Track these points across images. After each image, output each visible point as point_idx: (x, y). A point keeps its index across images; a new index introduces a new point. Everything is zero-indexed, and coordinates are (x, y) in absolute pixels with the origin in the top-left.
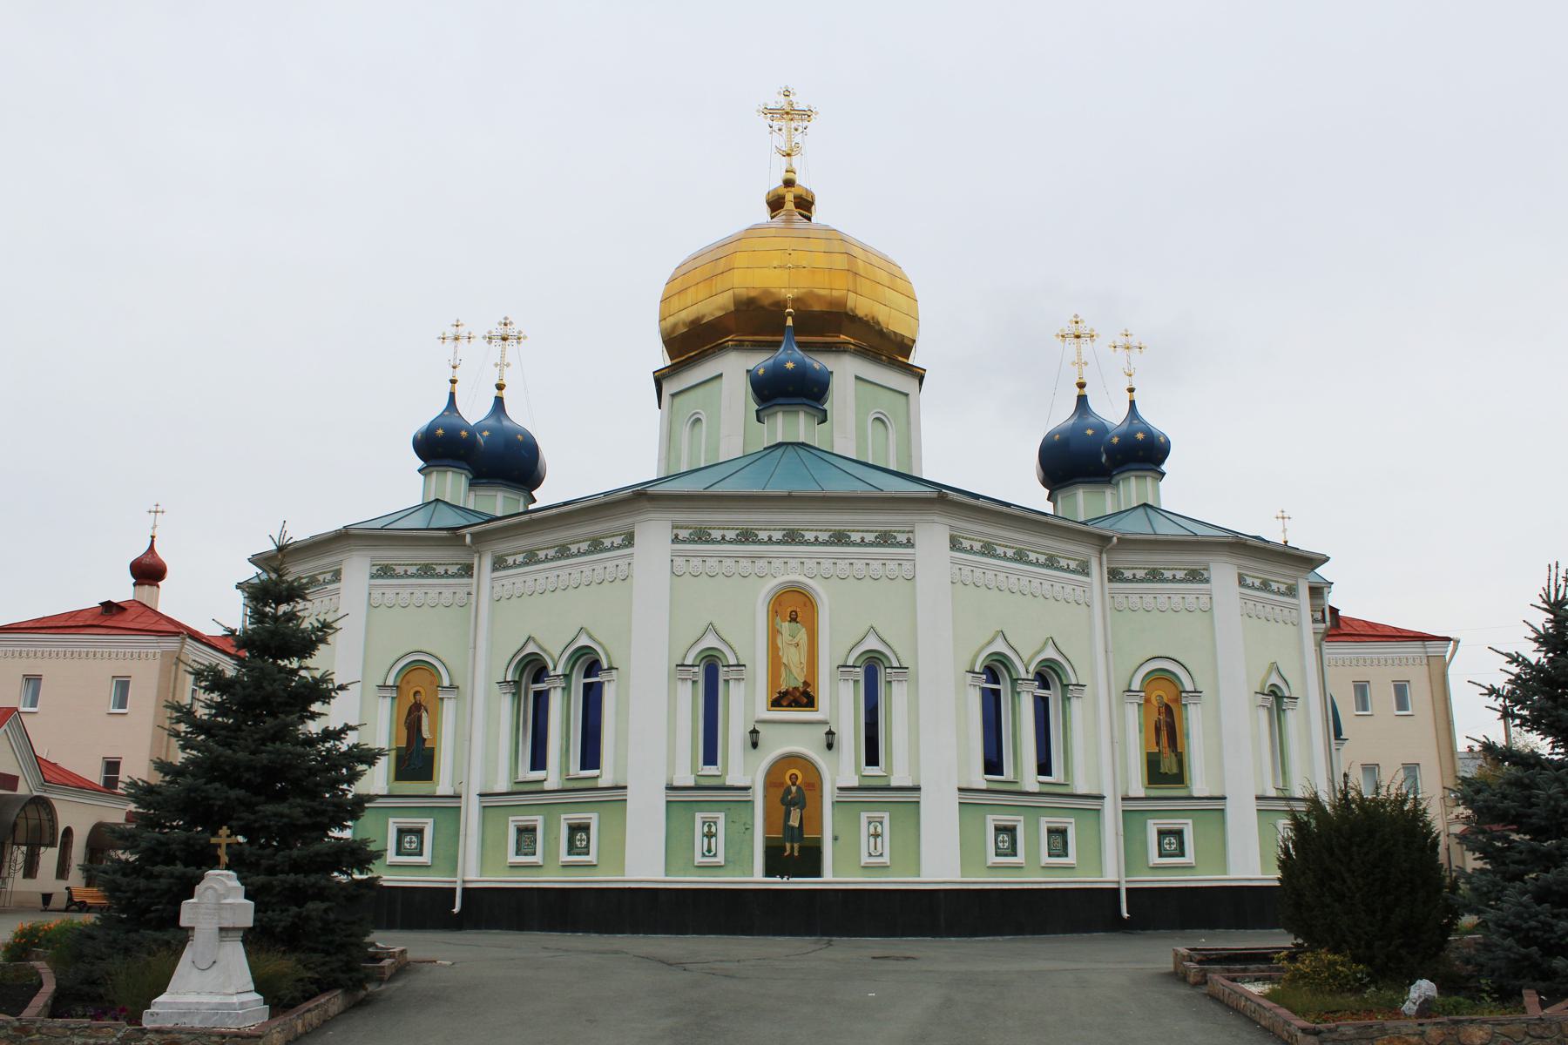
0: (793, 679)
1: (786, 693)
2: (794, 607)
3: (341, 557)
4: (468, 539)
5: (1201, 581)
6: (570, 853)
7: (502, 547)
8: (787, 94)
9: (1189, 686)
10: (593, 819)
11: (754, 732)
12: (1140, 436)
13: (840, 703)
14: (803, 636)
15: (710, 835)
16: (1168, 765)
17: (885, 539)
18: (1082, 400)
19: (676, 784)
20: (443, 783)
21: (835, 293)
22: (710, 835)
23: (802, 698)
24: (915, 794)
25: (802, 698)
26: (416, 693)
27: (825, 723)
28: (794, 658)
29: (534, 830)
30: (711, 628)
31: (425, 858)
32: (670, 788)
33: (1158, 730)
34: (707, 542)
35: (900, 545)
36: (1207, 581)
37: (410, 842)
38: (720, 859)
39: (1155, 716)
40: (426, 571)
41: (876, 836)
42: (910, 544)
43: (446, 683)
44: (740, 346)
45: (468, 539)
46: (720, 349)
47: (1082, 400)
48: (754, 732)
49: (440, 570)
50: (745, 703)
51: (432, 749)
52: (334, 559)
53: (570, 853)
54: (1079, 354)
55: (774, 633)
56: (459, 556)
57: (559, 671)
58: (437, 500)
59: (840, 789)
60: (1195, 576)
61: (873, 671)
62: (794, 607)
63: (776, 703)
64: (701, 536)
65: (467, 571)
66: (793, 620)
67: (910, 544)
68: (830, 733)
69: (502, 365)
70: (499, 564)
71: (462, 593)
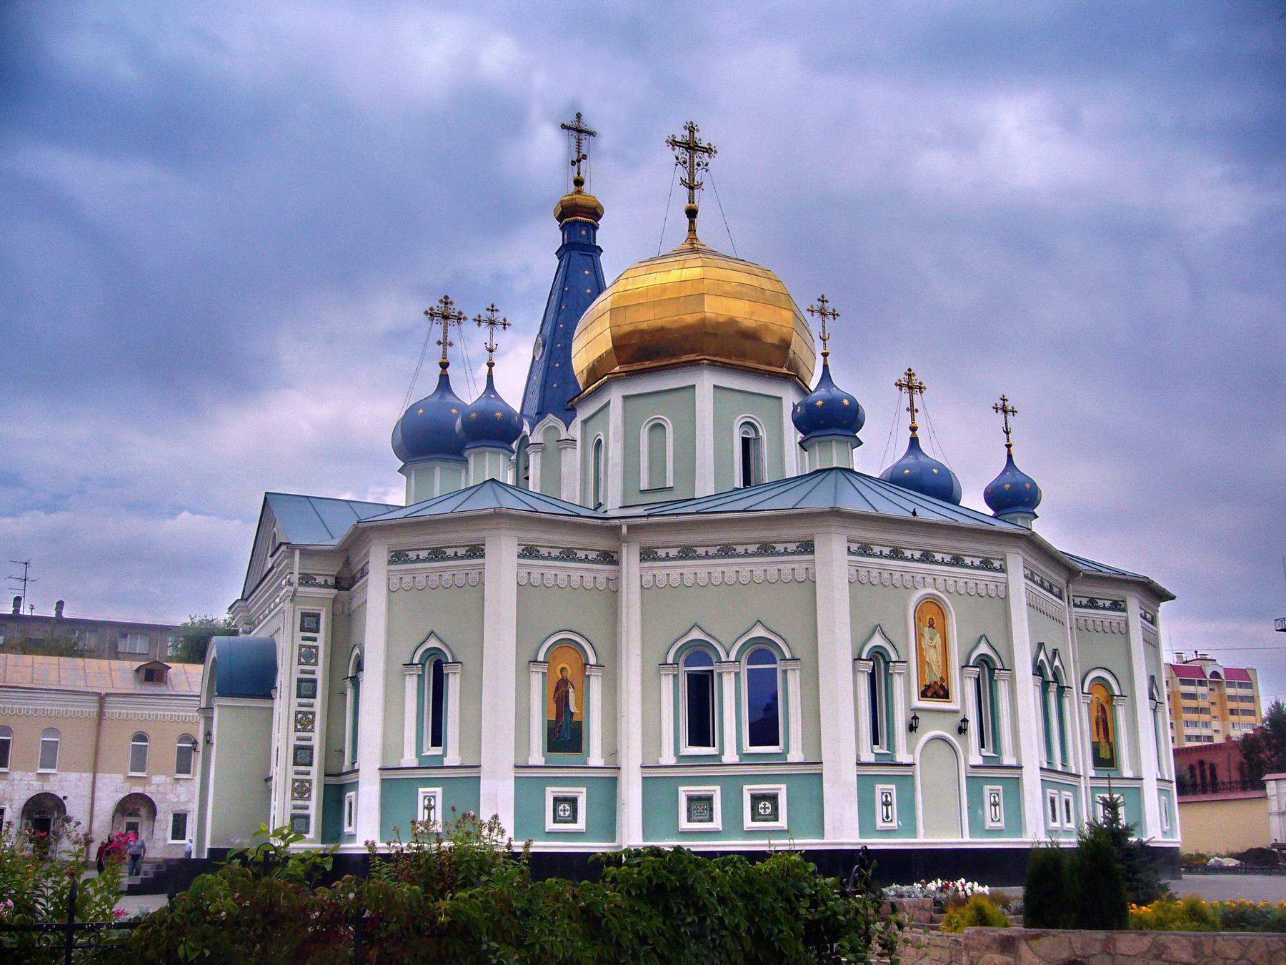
0: (935, 675)
1: (929, 687)
2: (932, 614)
3: (485, 534)
4: (624, 529)
5: (1120, 610)
6: (753, 820)
7: (651, 540)
8: (692, 129)
9: (1117, 692)
10: (716, 791)
11: (915, 718)
12: (1028, 486)
13: (963, 696)
14: (938, 639)
15: (887, 804)
16: (1104, 753)
17: (986, 565)
18: (914, 442)
19: (863, 760)
20: (596, 757)
21: (785, 330)
22: (887, 804)
23: (937, 690)
24: (1018, 771)
25: (937, 690)
26: (563, 669)
27: (956, 712)
28: (933, 656)
29: (709, 799)
30: (878, 628)
31: (782, 823)
32: (859, 764)
33: (1097, 724)
34: (870, 555)
35: (995, 570)
36: (1124, 610)
37: (565, 810)
38: (894, 825)
39: (1095, 713)
40: (568, 555)
41: (995, 804)
42: (1002, 570)
43: (592, 660)
44: (713, 365)
45: (624, 529)
46: (694, 364)
47: (914, 442)
48: (915, 718)
49: (581, 554)
50: (904, 695)
51: (580, 723)
52: (478, 534)
53: (753, 820)
54: (912, 401)
55: (919, 636)
56: (604, 543)
57: (732, 658)
58: (493, 480)
59: (973, 767)
60: (1117, 606)
61: (988, 671)
62: (932, 614)
63: (924, 695)
64: (865, 550)
65: (610, 558)
66: (931, 626)
67: (1002, 570)
68: (965, 721)
69: (445, 343)
70: (647, 555)
71: (601, 580)
